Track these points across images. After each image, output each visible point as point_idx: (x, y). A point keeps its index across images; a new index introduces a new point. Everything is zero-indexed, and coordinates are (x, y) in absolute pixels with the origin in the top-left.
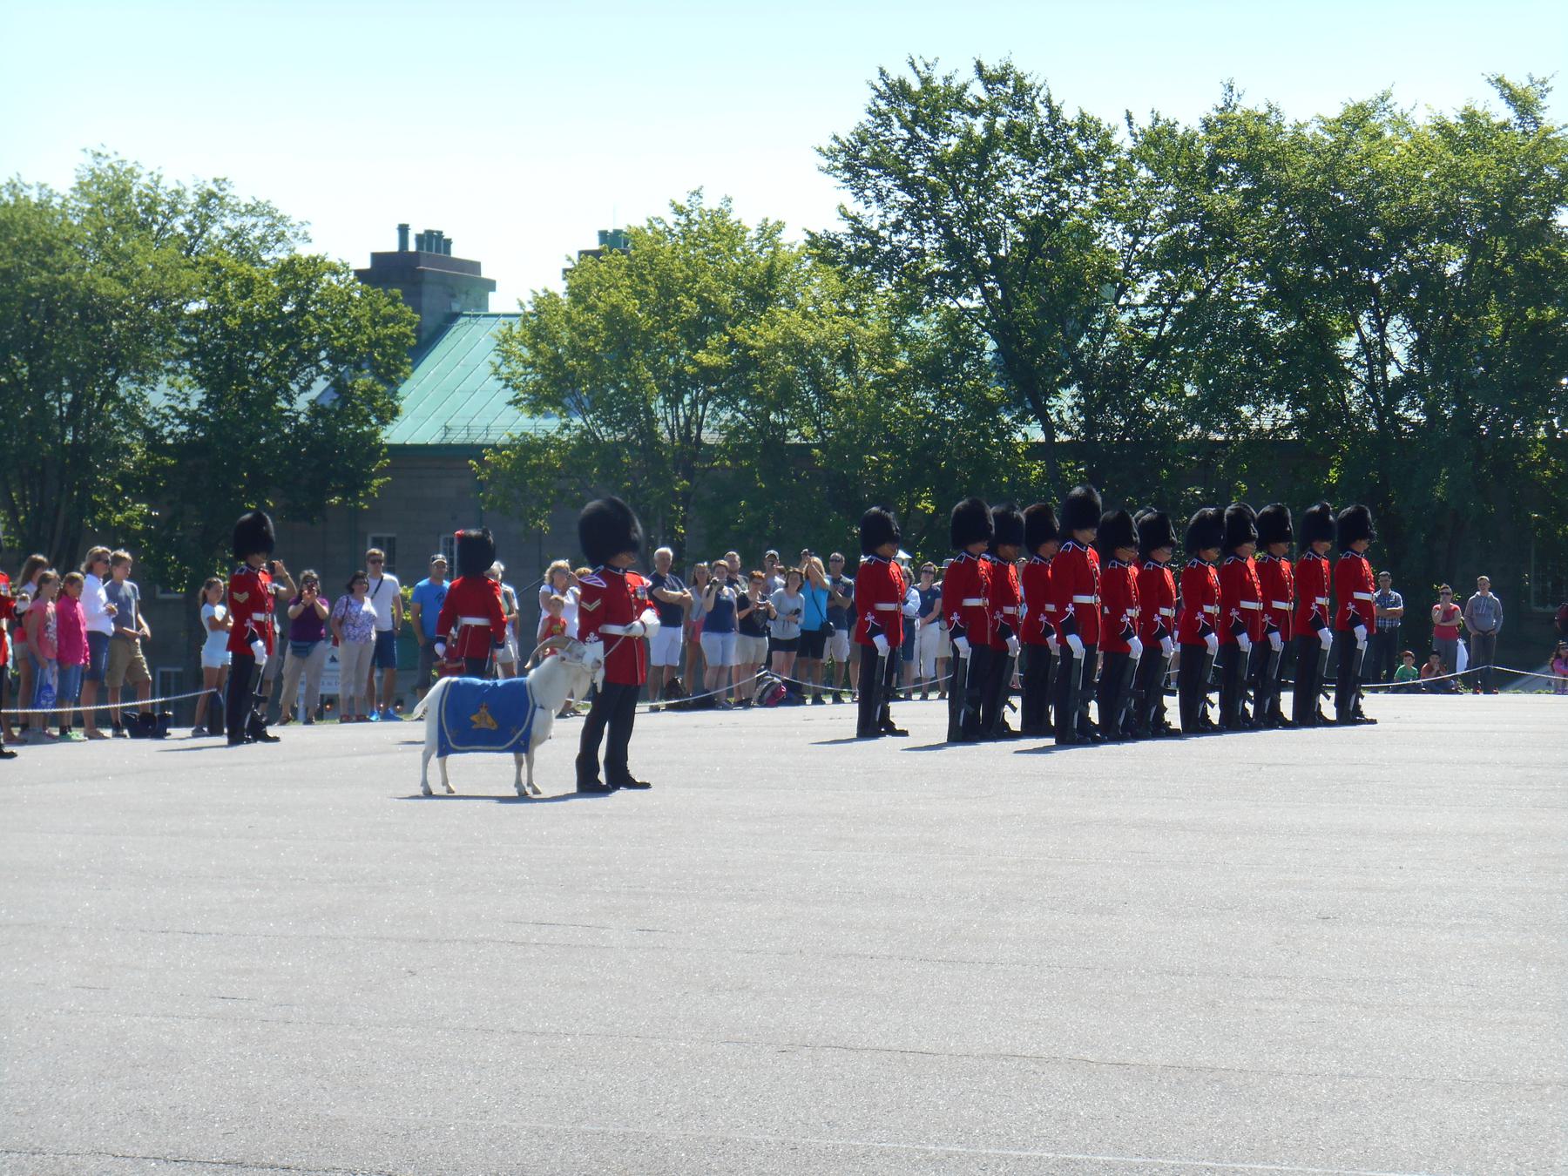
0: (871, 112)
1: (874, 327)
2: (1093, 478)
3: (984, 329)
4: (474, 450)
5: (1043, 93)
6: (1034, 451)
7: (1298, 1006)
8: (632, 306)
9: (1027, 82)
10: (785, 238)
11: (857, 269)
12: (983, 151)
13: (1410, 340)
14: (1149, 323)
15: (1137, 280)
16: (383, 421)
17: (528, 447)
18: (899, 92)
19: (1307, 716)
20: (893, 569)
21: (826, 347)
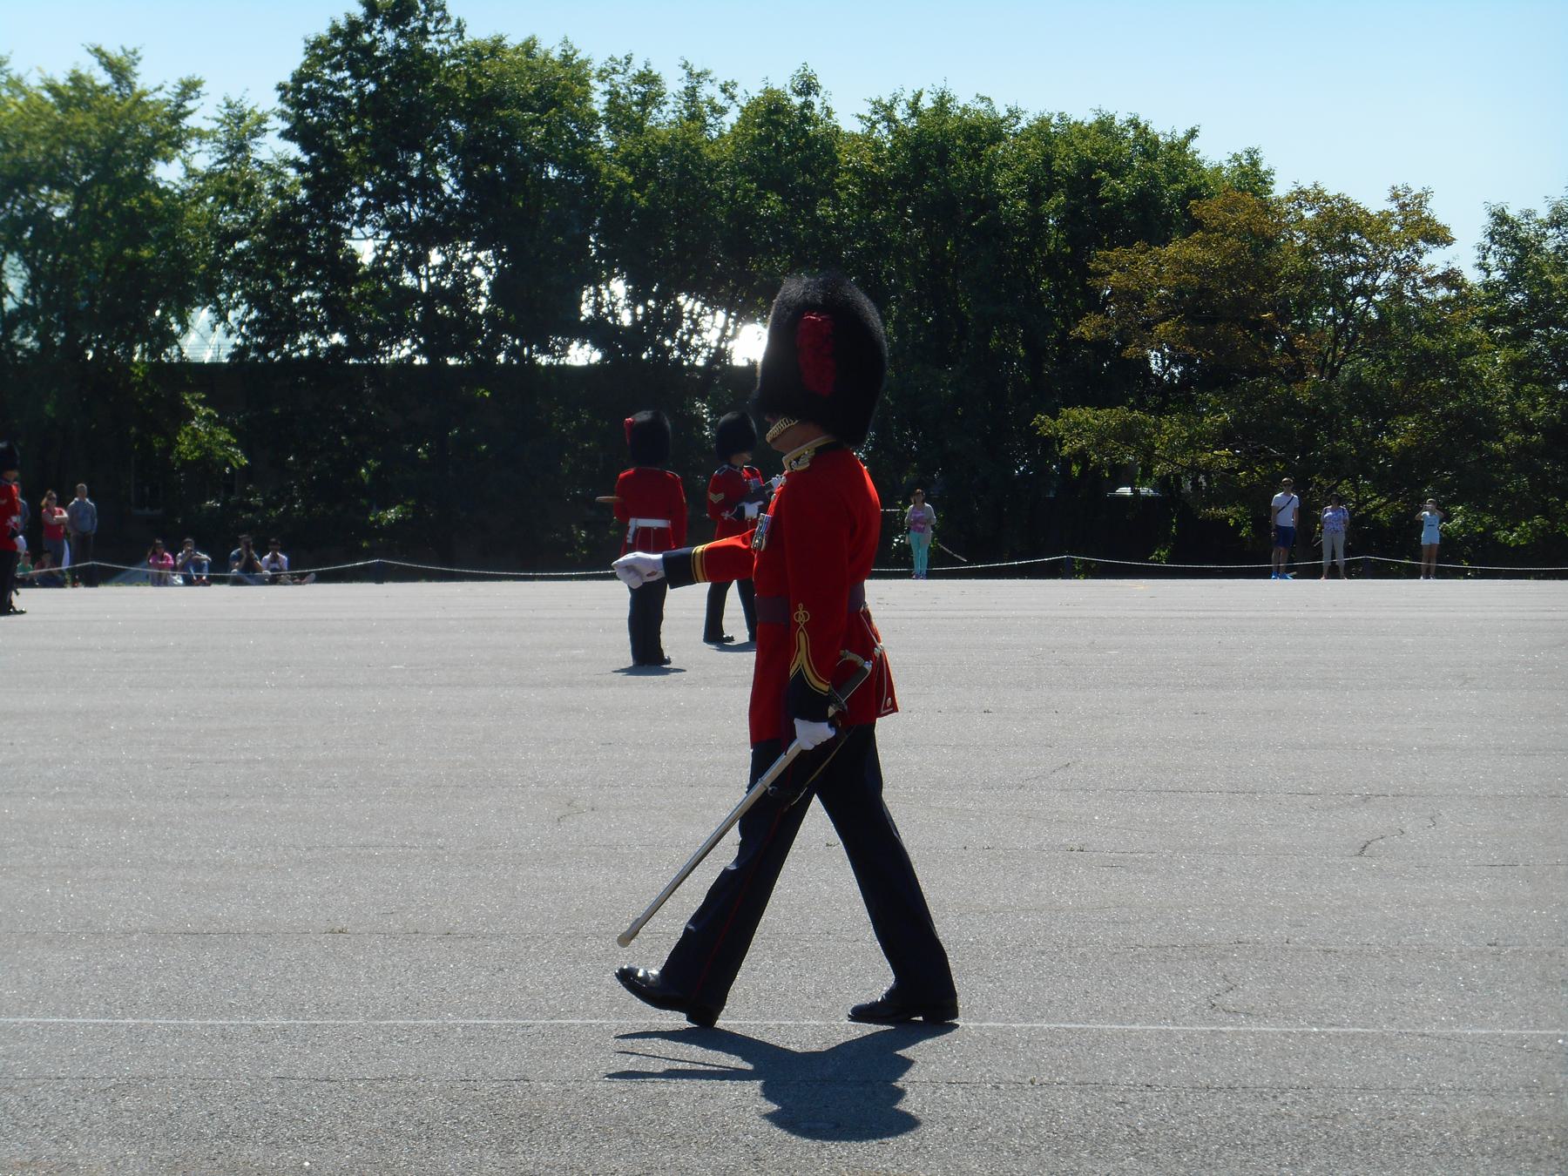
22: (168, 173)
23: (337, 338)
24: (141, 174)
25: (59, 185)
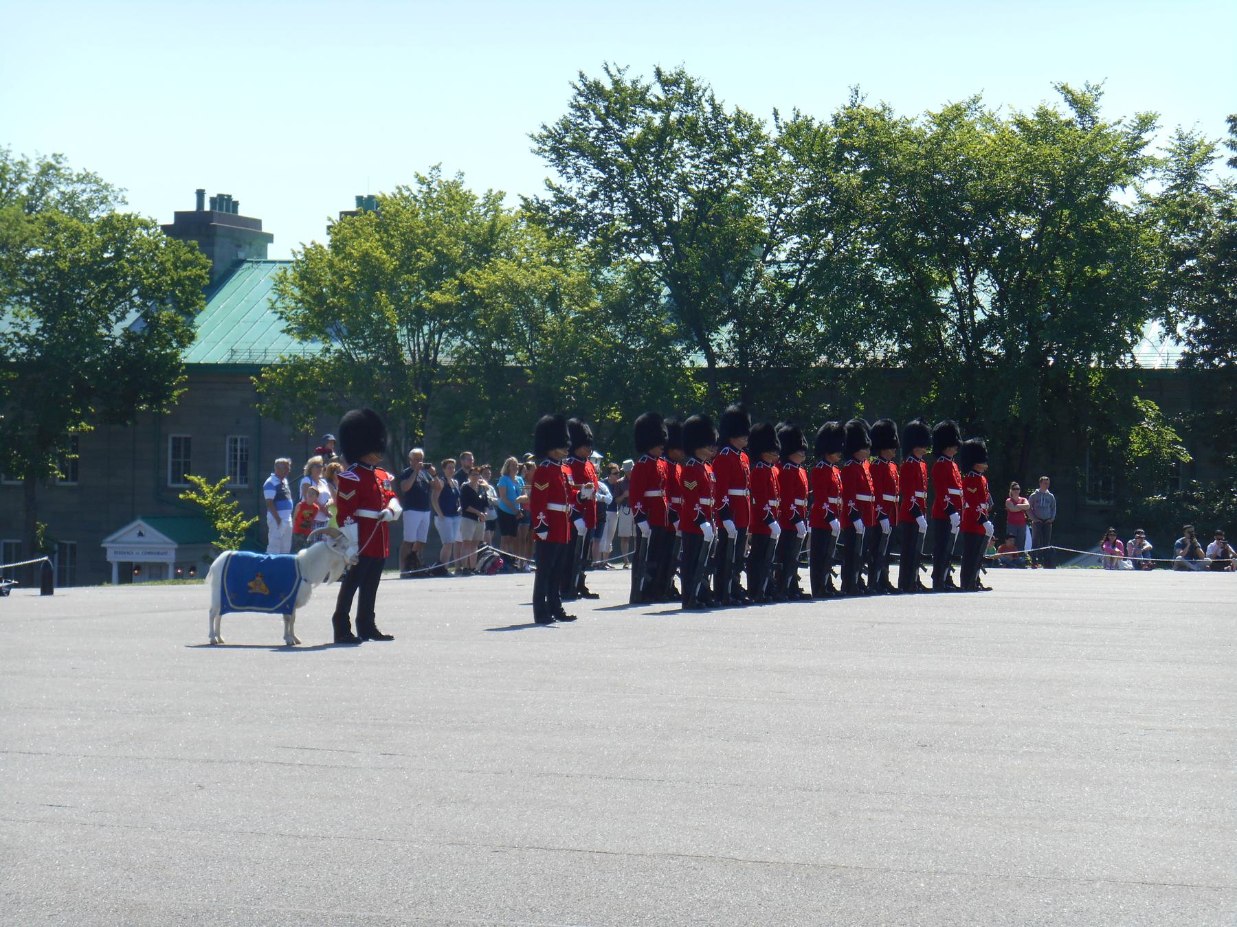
0: (573, 106)
1: (575, 276)
2: (744, 397)
3: (661, 279)
4: (254, 369)
5: (708, 93)
6: (700, 374)
7: (902, 816)
8: (380, 254)
9: (695, 85)
10: (505, 204)
11: (561, 230)
12: (661, 136)
13: (994, 291)
14: (790, 275)
15: (781, 241)
16: (182, 345)
17: (299, 366)
18: (594, 91)
19: (910, 585)
20: (588, 467)
21: (534, 291)
22: (1123, 198)
24: (1099, 200)
25: (1027, 211)
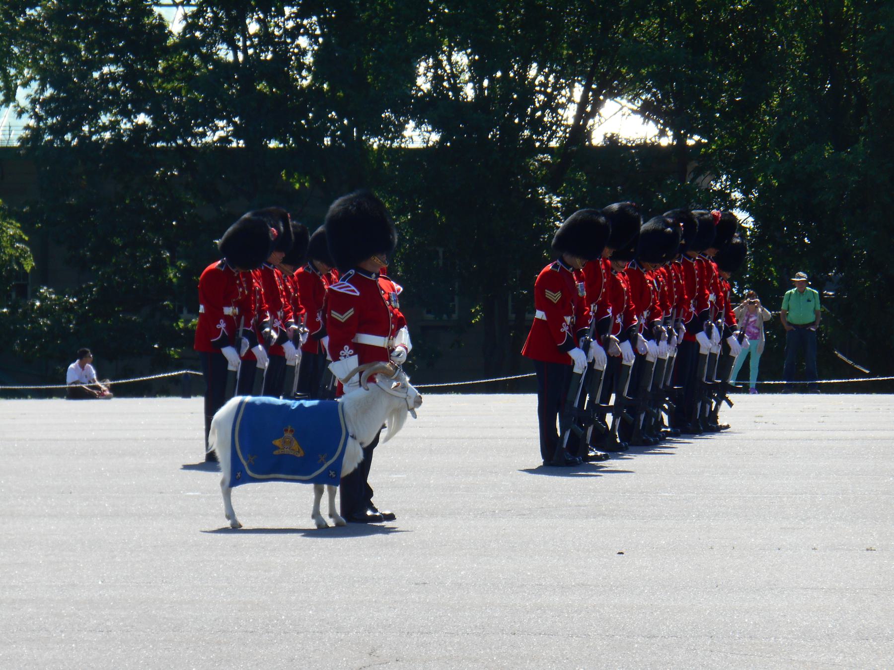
23: (142, 118)
